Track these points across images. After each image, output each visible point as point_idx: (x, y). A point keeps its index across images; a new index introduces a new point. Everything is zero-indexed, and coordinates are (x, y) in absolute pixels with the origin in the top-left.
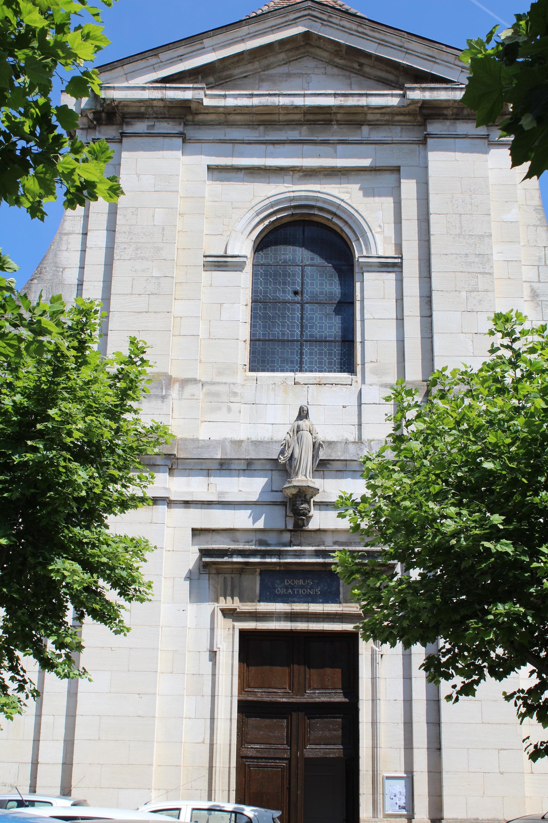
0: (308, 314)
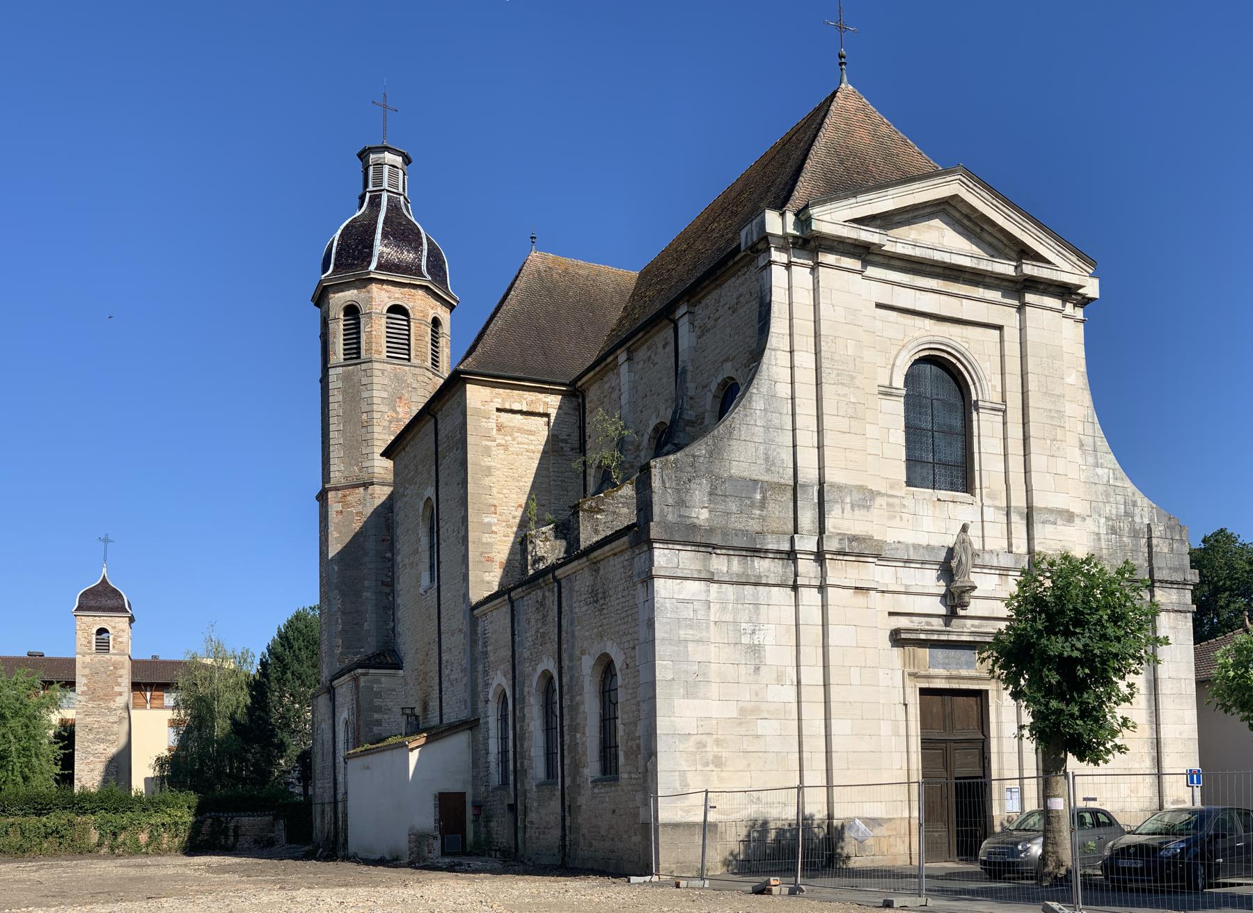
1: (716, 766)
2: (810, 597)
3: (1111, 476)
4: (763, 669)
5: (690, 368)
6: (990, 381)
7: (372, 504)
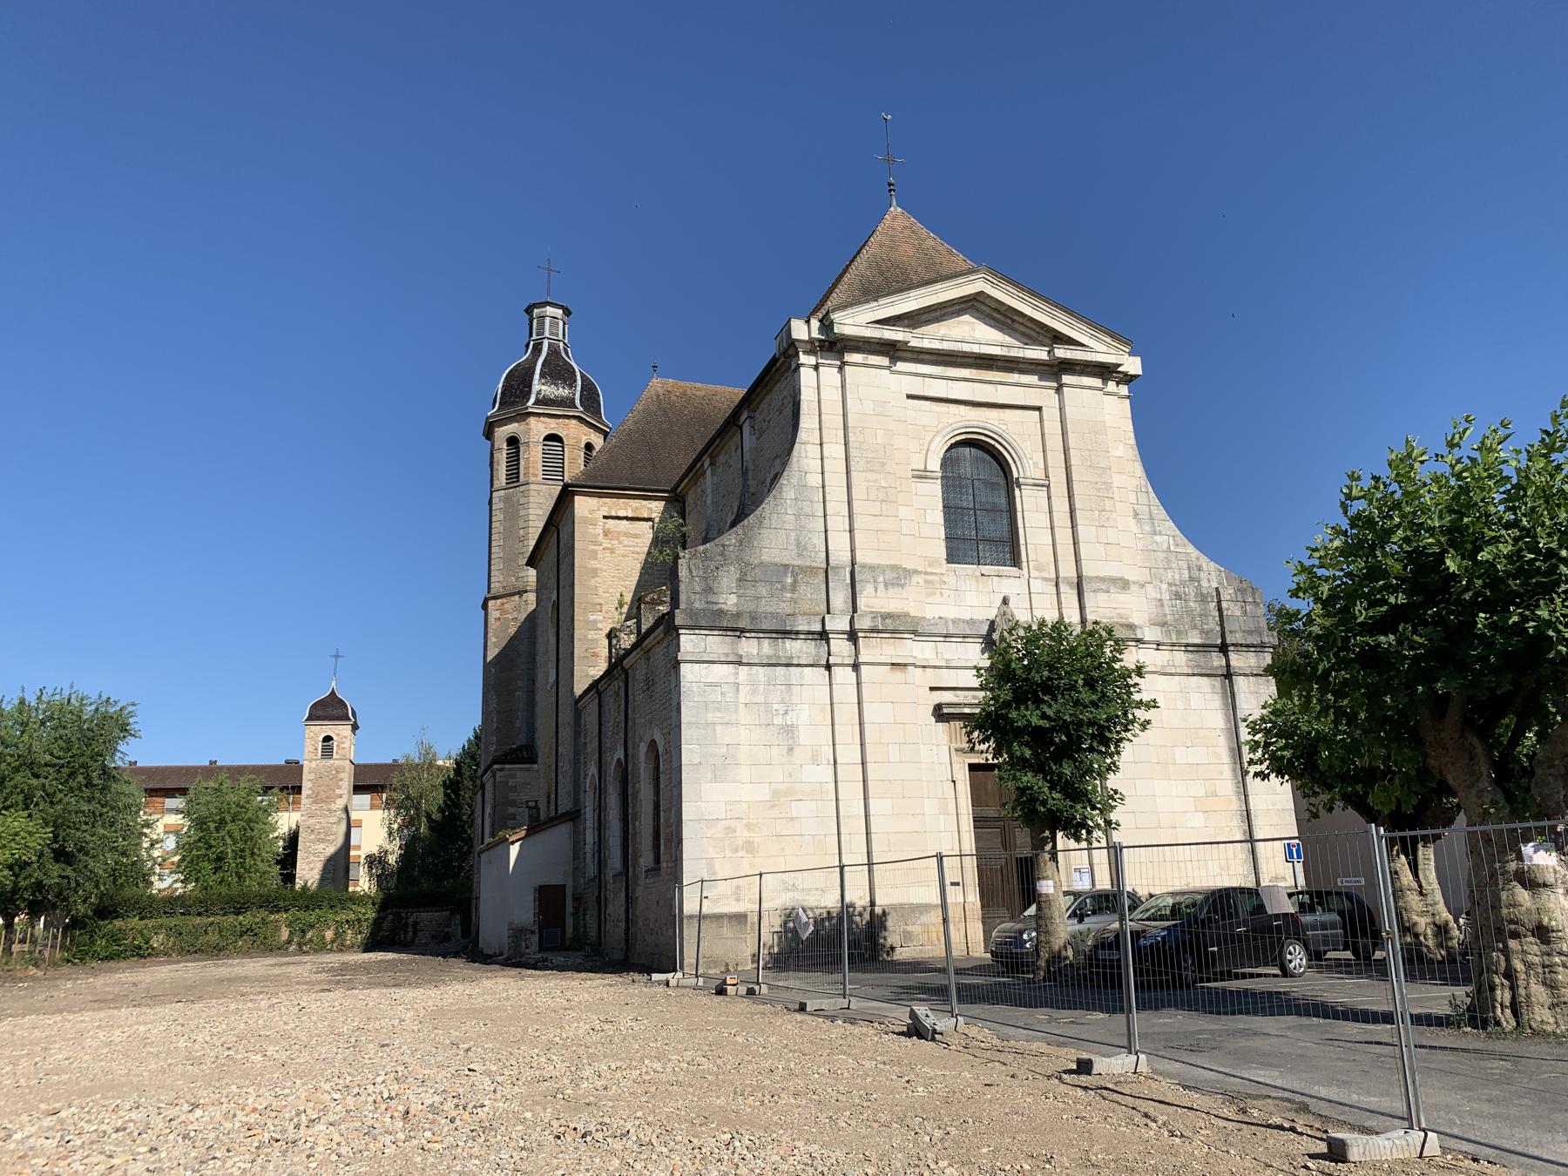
0: (979, 519)
1: (747, 852)
2: (844, 675)
3: (1171, 542)
4: (797, 750)
5: (751, 467)
6: (1032, 459)
7: (526, 610)
